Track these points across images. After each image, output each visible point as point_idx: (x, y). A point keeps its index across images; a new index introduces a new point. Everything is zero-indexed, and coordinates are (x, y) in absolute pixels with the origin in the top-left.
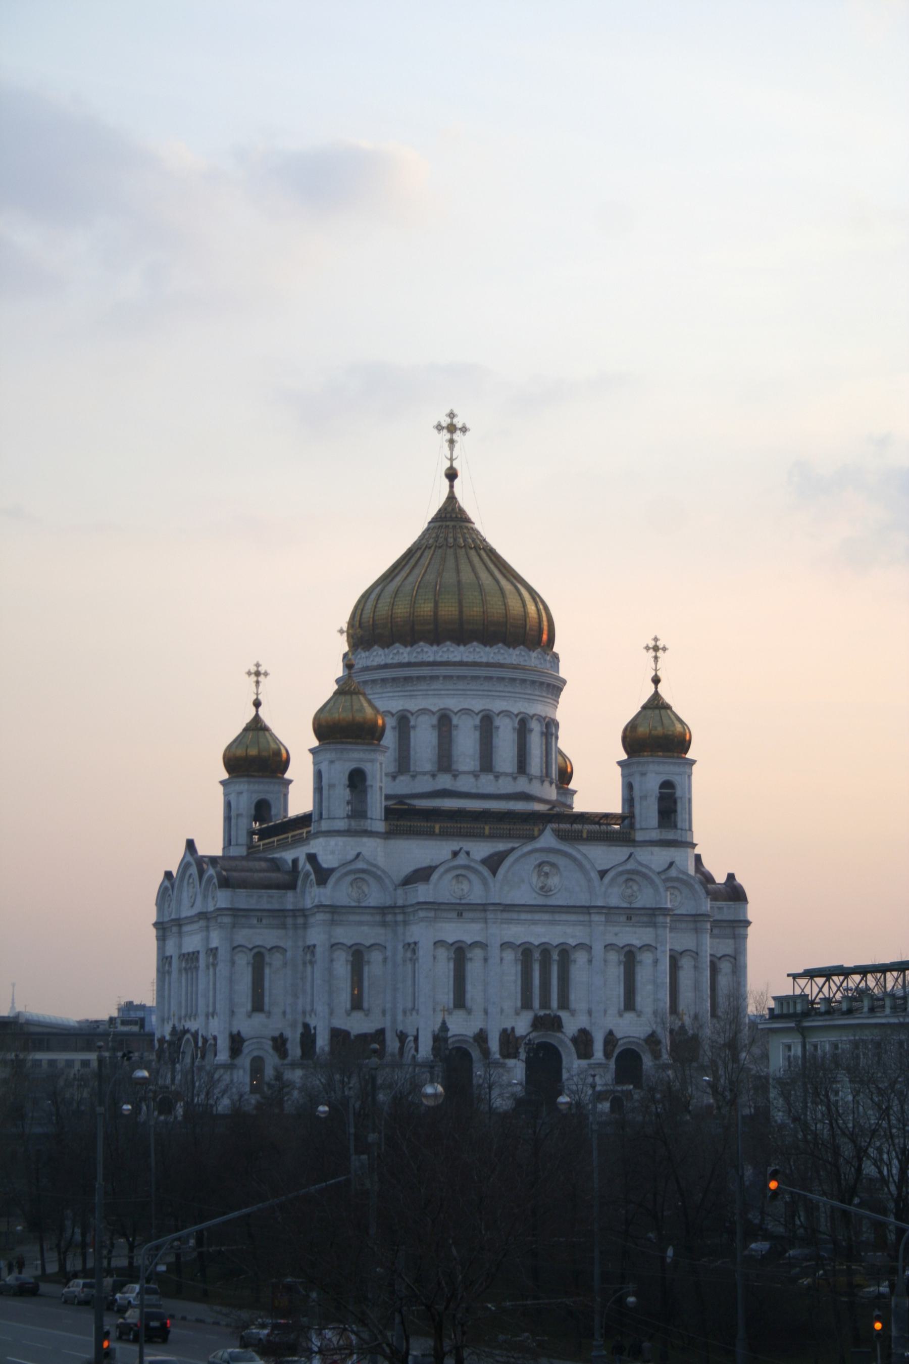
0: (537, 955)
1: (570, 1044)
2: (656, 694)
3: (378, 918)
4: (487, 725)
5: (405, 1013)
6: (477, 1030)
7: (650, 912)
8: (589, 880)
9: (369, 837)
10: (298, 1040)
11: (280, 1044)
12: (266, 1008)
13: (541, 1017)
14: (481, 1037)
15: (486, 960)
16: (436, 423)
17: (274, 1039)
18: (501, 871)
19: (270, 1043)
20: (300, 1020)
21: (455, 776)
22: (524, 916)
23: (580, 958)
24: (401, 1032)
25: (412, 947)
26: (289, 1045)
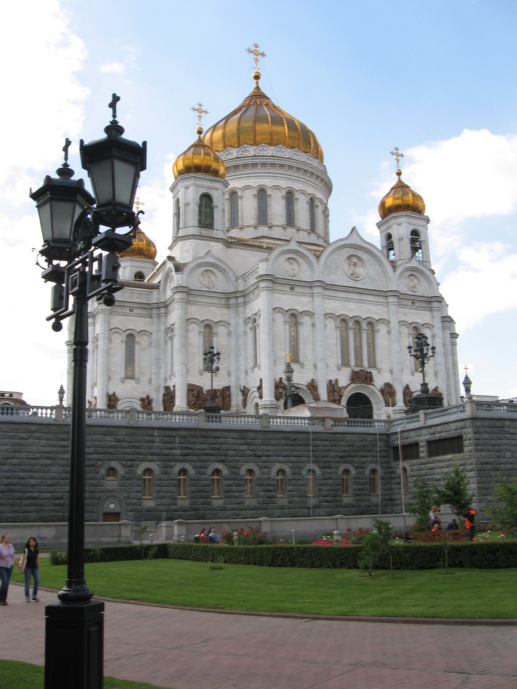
0: (351, 324)
1: (380, 394)
2: (400, 181)
3: (223, 302)
4: (290, 197)
5: (246, 372)
6: (309, 381)
7: (427, 300)
8: (385, 272)
9: (217, 242)
10: (161, 399)
11: (146, 403)
12: (136, 376)
13: (357, 372)
14: (313, 386)
15: (313, 325)
16: (247, 48)
17: (142, 400)
18: (323, 258)
19: (139, 402)
20: (163, 385)
21: (270, 227)
22: (340, 294)
23: (382, 329)
24: (244, 387)
25: (253, 321)
26: (154, 405)
